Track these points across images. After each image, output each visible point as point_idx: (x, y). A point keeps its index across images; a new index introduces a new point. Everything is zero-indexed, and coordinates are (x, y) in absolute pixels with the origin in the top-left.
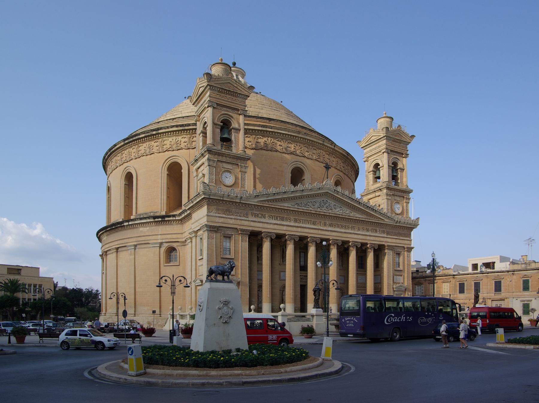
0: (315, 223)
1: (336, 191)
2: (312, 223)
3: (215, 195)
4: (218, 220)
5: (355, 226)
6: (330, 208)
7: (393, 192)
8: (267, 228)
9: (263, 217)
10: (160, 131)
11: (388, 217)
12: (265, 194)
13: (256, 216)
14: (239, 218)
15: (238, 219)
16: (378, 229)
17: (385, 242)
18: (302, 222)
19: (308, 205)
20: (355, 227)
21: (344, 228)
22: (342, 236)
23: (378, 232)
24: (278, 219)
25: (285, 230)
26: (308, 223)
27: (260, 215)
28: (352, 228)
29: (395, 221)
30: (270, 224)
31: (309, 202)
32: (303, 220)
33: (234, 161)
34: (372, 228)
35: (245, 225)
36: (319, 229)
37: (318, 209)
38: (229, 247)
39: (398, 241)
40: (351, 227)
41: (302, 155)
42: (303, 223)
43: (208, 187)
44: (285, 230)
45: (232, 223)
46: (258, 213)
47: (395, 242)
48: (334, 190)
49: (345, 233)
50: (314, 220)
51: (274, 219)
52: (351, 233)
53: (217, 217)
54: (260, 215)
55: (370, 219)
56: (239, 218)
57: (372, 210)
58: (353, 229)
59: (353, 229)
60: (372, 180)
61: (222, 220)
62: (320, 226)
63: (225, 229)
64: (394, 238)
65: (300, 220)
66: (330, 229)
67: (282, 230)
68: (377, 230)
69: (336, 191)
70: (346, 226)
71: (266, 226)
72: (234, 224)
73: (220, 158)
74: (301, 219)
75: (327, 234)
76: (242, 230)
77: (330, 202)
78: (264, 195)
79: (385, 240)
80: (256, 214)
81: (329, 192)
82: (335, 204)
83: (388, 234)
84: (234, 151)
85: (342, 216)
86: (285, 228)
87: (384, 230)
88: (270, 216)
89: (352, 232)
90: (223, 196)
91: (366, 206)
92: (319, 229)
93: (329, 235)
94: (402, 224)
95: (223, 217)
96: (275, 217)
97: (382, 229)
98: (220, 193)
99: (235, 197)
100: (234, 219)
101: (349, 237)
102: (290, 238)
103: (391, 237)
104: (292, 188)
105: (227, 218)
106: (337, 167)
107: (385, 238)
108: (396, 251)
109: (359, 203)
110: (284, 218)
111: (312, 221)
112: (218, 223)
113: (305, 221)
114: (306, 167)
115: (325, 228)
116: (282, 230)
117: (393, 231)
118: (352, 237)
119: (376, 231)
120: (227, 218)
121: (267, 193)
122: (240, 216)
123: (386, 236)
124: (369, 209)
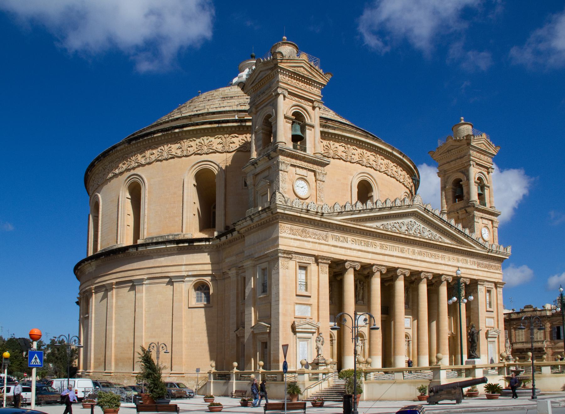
2: (399, 251)
3: (292, 208)
4: (293, 243)
5: (445, 254)
6: (418, 231)
8: (350, 255)
9: (345, 242)
10: (185, 129)
12: (349, 210)
13: (337, 239)
14: (317, 241)
15: (316, 243)
16: (468, 259)
17: (476, 275)
18: (388, 249)
19: (395, 227)
21: (434, 257)
22: (432, 268)
23: (469, 264)
24: (363, 244)
25: (370, 259)
26: (396, 250)
27: (341, 239)
28: (442, 257)
30: (354, 250)
32: (390, 247)
33: (310, 166)
35: (325, 251)
37: (405, 232)
38: (304, 281)
39: (489, 275)
40: (441, 256)
41: (369, 165)
42: (390, 250)
43: (283, 199)
44: (370, 259)
45: (309, 248)
46: (339, 235)
47: (487, 276)
48: (424, 209)
49: (435, 263)
51: (357, 244)
52: (441, 264)
53: (291, 239)
54: (341, 239)
56: (317, 241)
59: (443, 259)
60: (451, 199)
61: (297, 243)
62: (408, 254)
63: (301, 256)
65: (386, 246)
66: (419, 258)
67: (367, 259)
70: (436, 255)
71: (349, 252)
72: (312, 250)
73: (294, 161)
74: (387, 245)
76: (324, 258)
77: (419, 224)
78: (349, 211)
80: (337, 237)
81: (419, 211)
82: (424, 226)
83: (479, 265)
84: (310, 152)
86: (370, 256)
88: (353, 240)
89: (443, 262)
90: (301, 211)
93: (418, 266)
95: (299, 240)
96: (359, 241)
98: (298, 207)
99: (315, 213)
100: (313, 242)
101: (439, 269)
102: (377, 269)
104: (360, 206)
105: (303, 241)
106: (404, 182)
107: (476, 271)
108: (487, 287)
110: (369, 243)
111: (400, 248)
112: (293, 247)
114: (375, 180)
115: (414, 257)
116: (367, 259)
119: (467, 262)
120: (303, 241)
121: (351, 209)
122: (319, 239)
123: (477, 268)
124: (461, 233)
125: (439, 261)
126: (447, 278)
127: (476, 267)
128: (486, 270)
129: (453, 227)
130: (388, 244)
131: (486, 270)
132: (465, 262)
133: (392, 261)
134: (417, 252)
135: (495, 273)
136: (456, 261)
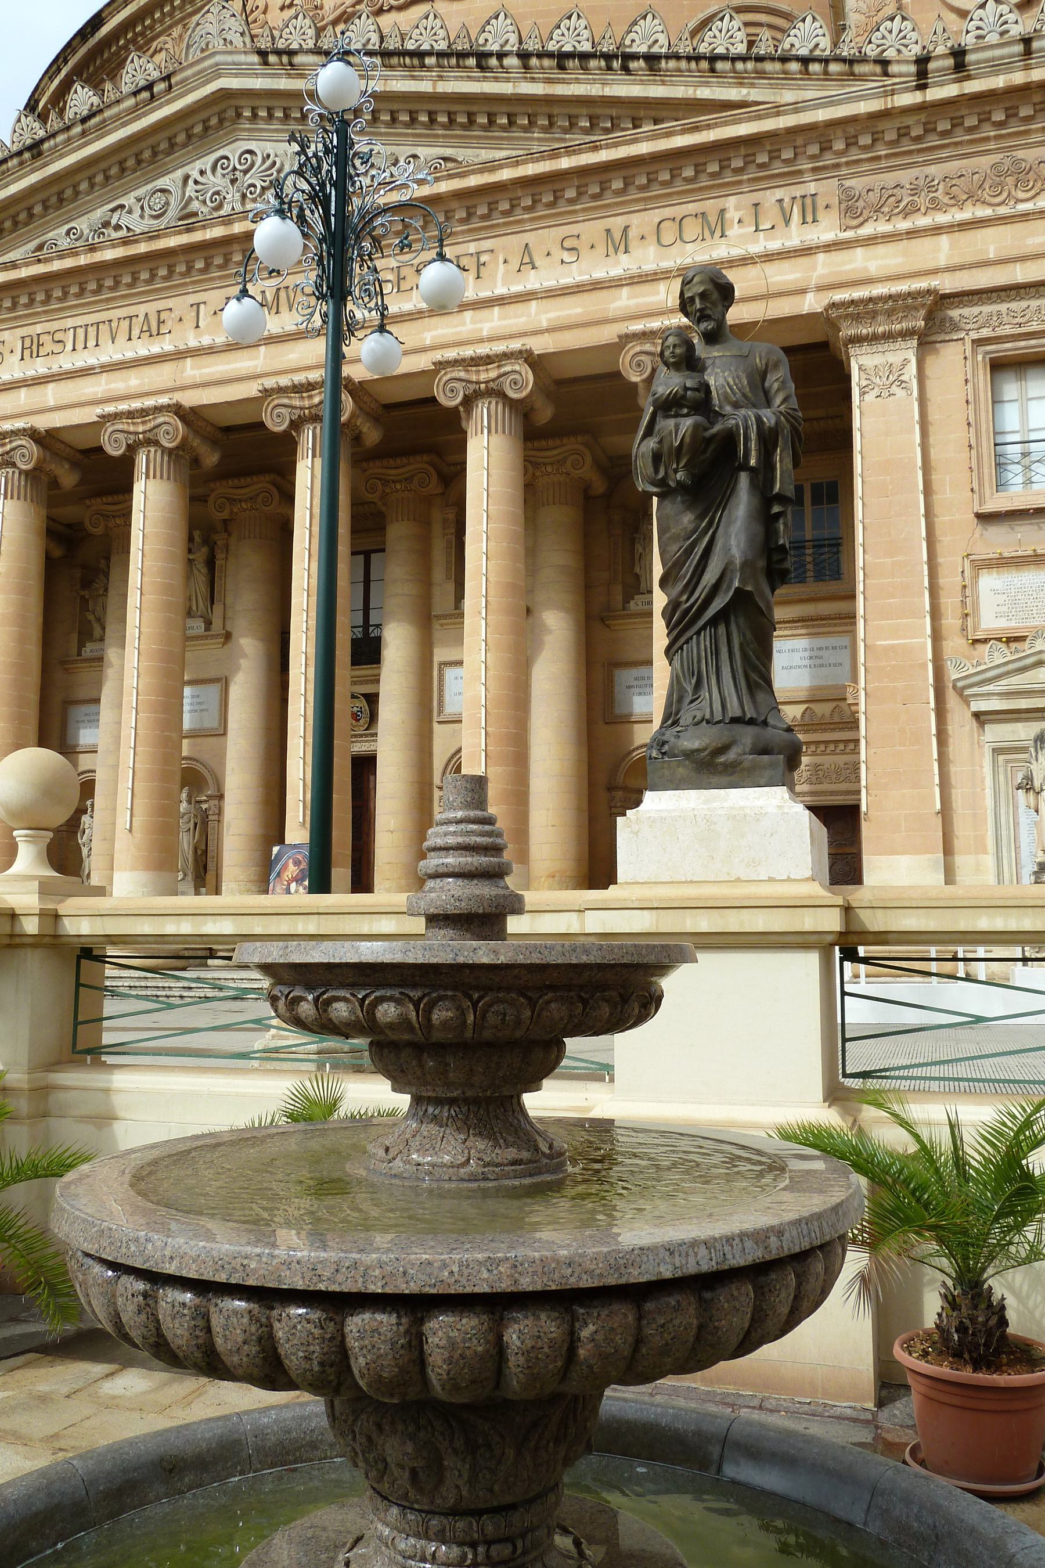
0: (160, 322)
1: (272, 59)
5: (487, 244)
11: (794, 66)
16: (731, 202)
18: (69, 346)
20: (484, 258)
29: (893, 69)
31: (122, 207)
34: (668, 212)
36: (179, 355)
42: (80, 345)
50: (151, 308)
55: (595, 148)
57: (616, 64)
65: (57, 337)
68: (723, 211)
69: (272, 59)
70: (404, 272)
75: (244, 373)
79: (823, 267)
87: (812, 188)
91: (546, 62)
92: (179, 355)
94: (996, 67)
97: (779, 193)
101: (428, 342)
107: (821, 257)
109: (472, 62)
111: (142, 318)
113: (92, 331)
117: (932, 170)
118: (457, 338)
126: (483, 377)
127: (826, 231)
129: (501, 56)
130: (70, 323)
132: (692, 229)
133: (83, 399)
136: (601, 249)
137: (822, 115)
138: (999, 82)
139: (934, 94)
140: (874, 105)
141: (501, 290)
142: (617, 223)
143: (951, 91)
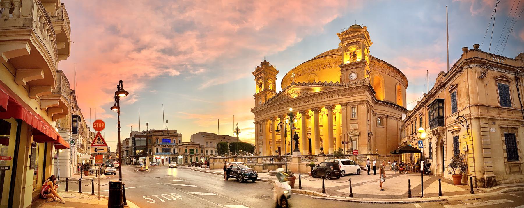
7: (348, 67)
16: (333, 95)
39: (351, 98)
40: (312, 100)
52: (311, 104)
58: (313, 101)
64: (348, 97)
66: (299, 105)
79: (340, 100)
85: (302, 97)
87: (339, 94)
103: (345, 97)
115: (296, 106)
119: (332, 97)
123: (340, 98)
125: (312, 102)
127: (340, 97)
128: (349, 96)
131: (349, 96)
134: (298, 103)
135: (358, 96)
137: (339, 89)
138: (351, 87)
139: (346, 88)
140: (342, 88)
141: (316, 102)
142: (324, 97)
143: (348, 87)
